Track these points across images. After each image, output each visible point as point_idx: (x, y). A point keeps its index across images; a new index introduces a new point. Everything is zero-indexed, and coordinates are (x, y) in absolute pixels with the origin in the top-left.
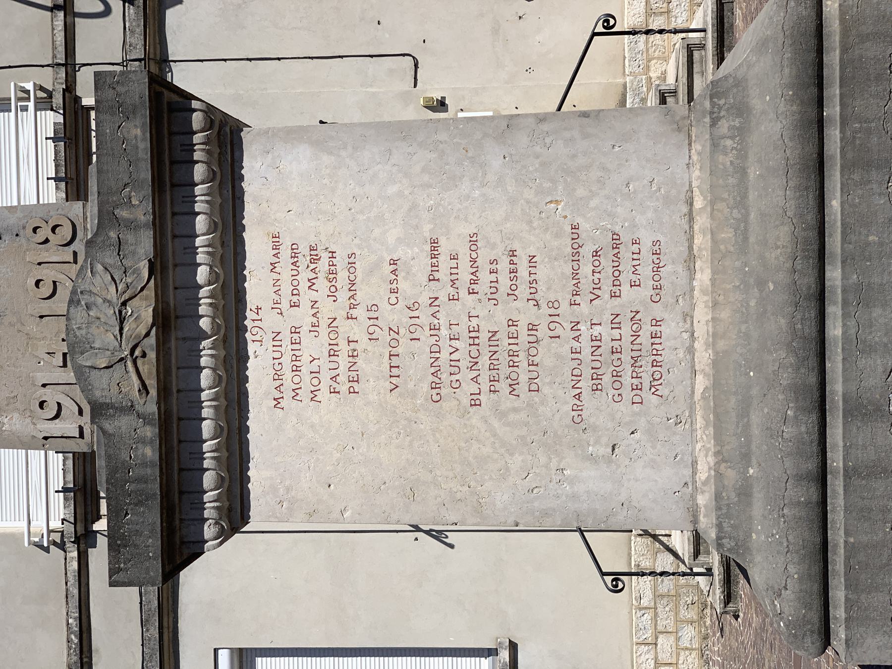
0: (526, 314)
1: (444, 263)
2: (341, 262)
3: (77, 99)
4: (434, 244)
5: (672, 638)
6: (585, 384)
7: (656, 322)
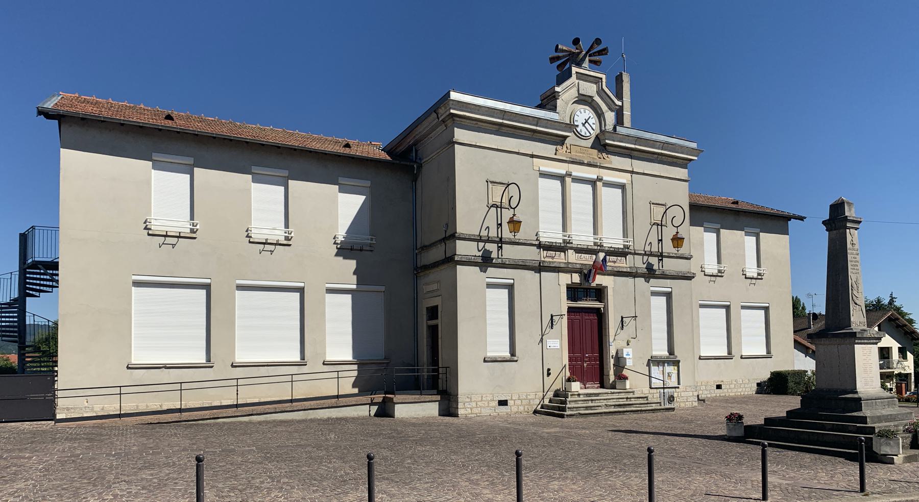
5: (520, 404)
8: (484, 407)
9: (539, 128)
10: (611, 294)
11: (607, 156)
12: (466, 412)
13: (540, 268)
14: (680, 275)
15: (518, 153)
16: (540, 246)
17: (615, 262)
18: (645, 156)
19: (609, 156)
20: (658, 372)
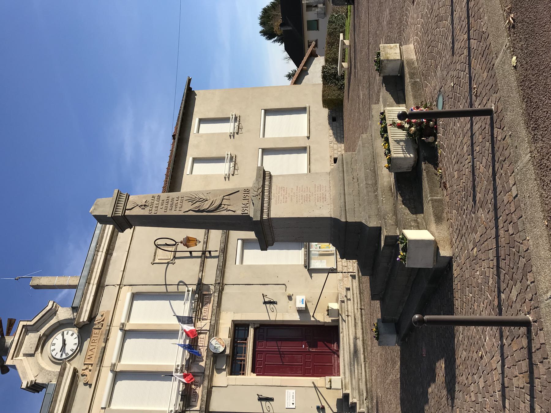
0: (309, 193)
1: (298, 188)
2: (285, 188)
4: (297, 187)
6: (316, 201)
7: (325, 194)
10: (240, 317)
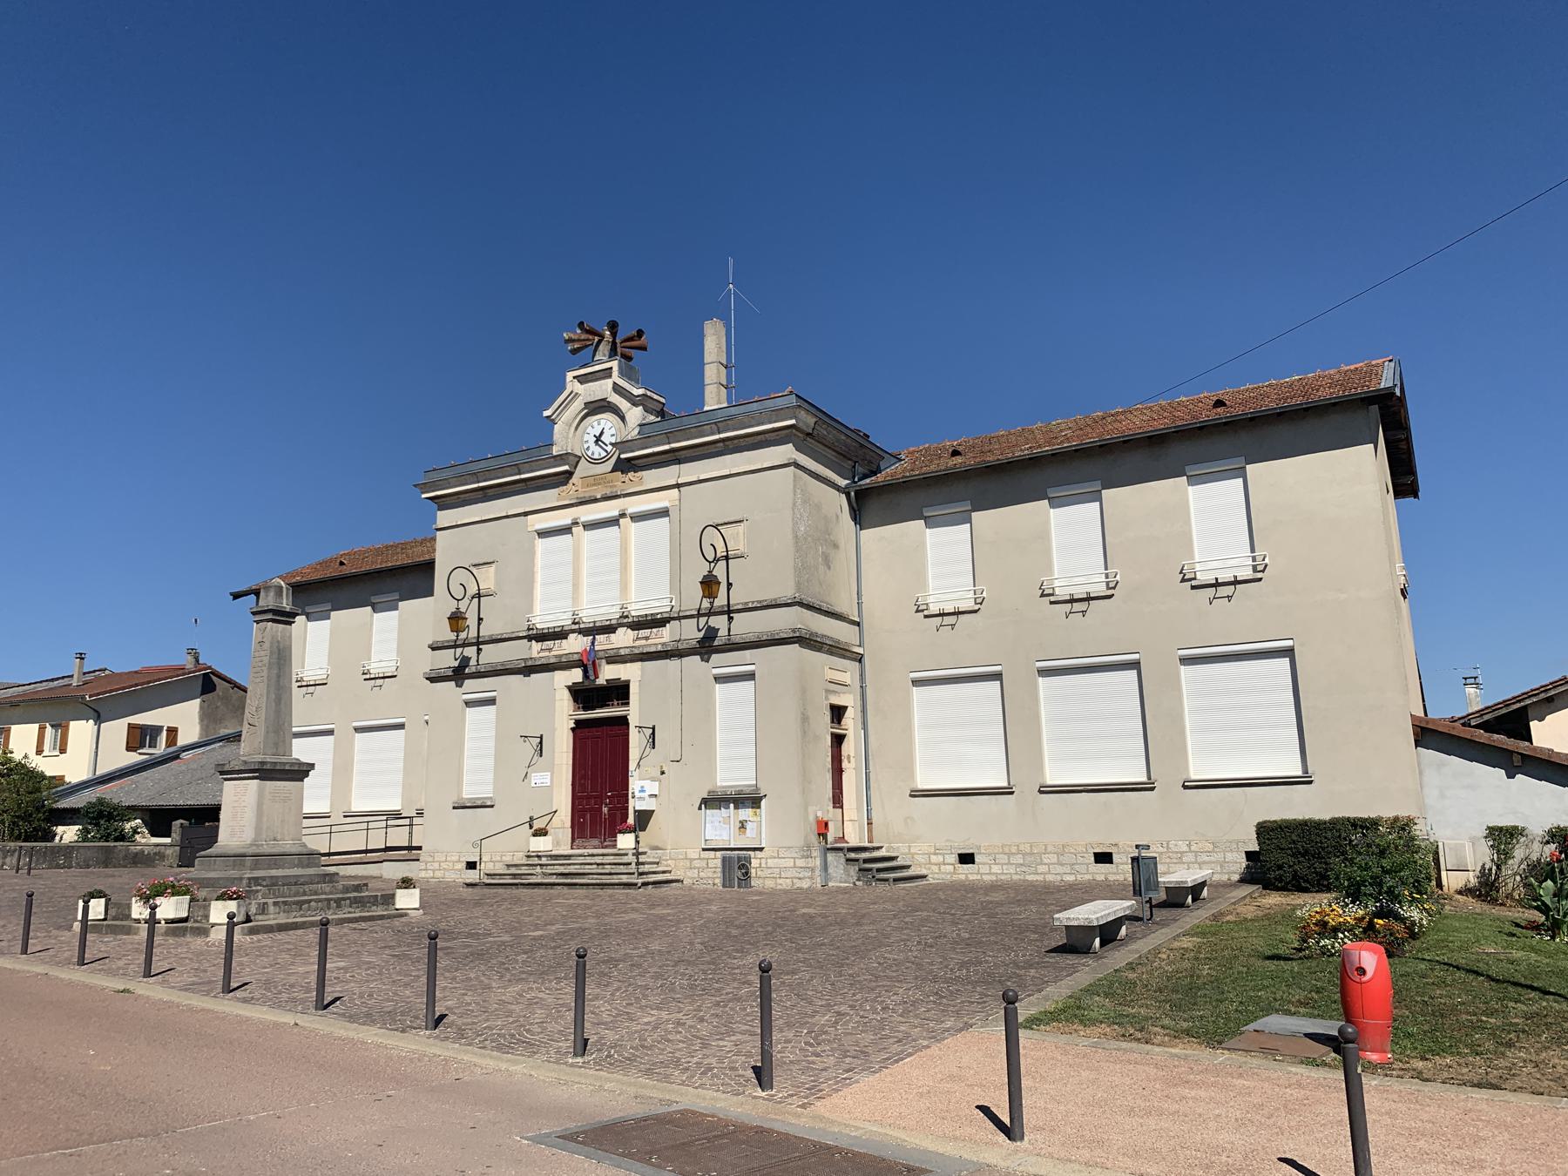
3: (669, 622)
8: (448, 870)
9: (523, 476)
11: (636, 474)
12: (427, 875)
13: (529, 669)
14: (765, 638)
15: (507, 517)
16: (530, 638)
17: (647, 638)
18: (712, 449)
19: (639, 474)
20: (722, 819)
